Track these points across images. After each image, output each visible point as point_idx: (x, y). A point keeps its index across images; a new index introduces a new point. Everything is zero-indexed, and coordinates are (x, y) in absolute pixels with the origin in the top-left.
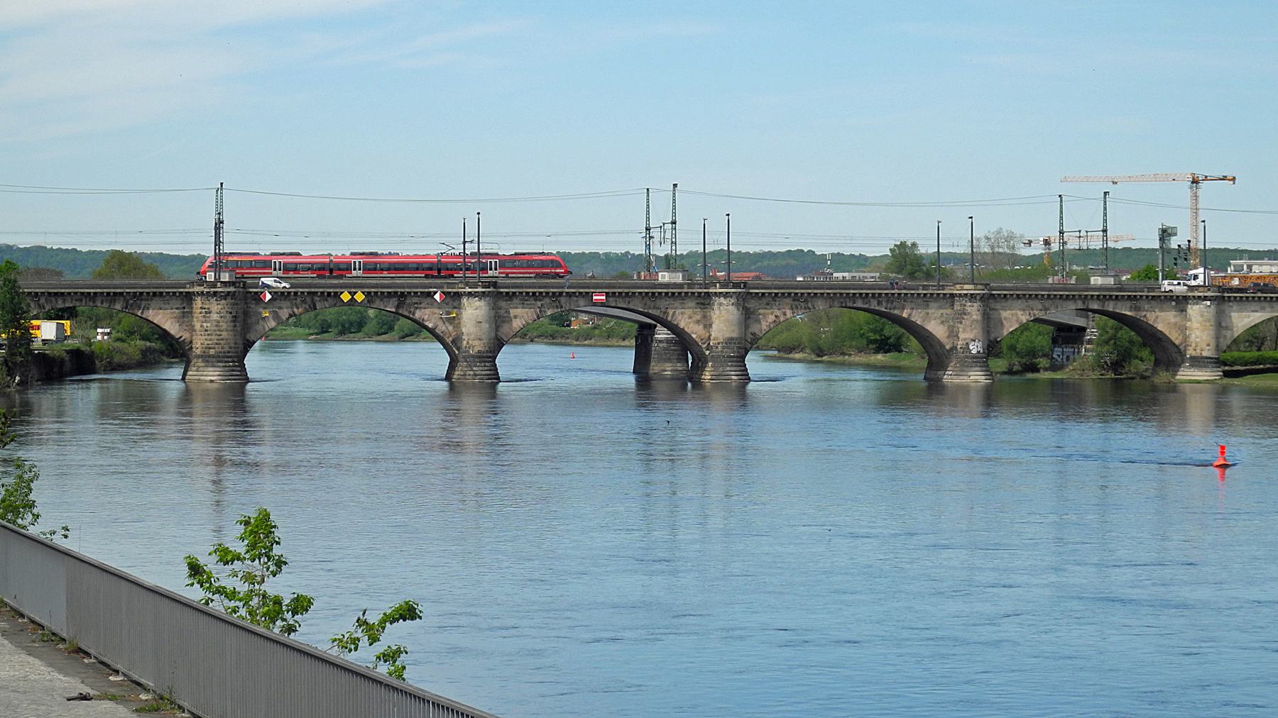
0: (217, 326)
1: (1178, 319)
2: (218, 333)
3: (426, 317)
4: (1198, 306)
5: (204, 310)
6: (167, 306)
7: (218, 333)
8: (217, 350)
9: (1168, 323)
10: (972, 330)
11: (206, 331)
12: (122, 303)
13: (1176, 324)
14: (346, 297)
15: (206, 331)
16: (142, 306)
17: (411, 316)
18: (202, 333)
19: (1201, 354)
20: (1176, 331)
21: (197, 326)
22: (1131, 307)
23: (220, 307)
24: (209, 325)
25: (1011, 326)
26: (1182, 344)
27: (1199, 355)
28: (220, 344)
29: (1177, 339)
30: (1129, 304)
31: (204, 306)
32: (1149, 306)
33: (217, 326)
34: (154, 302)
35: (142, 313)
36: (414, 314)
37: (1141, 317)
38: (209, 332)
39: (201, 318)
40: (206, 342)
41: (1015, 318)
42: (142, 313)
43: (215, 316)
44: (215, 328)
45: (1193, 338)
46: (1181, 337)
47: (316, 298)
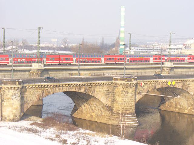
0: (131, 100)
2: (131, 103)
3: (191, 90)
5: (124, 92)
6: (102, 90)
7: (131, 103)
8: (130, 111)
11: (125, 102)
12: (84, 89)
14: (169, 83)
15: (125, 102)
16: (92, 90)
17: (186, 90)
18: (123, 103)
21: (119, 99)
23: (132, 90)
24: (127, 99)
28: (132, 108)
31: (124, 90)
33: (131, 100)
34: (97, 88)
35: (92, 93)
36: (187, 89)
38: (127, 103)
39: (122, 96)
40: (125, 108)
42: (92, 93)
43: (129, 95)
44: (130, 101)
47: (157, 84)
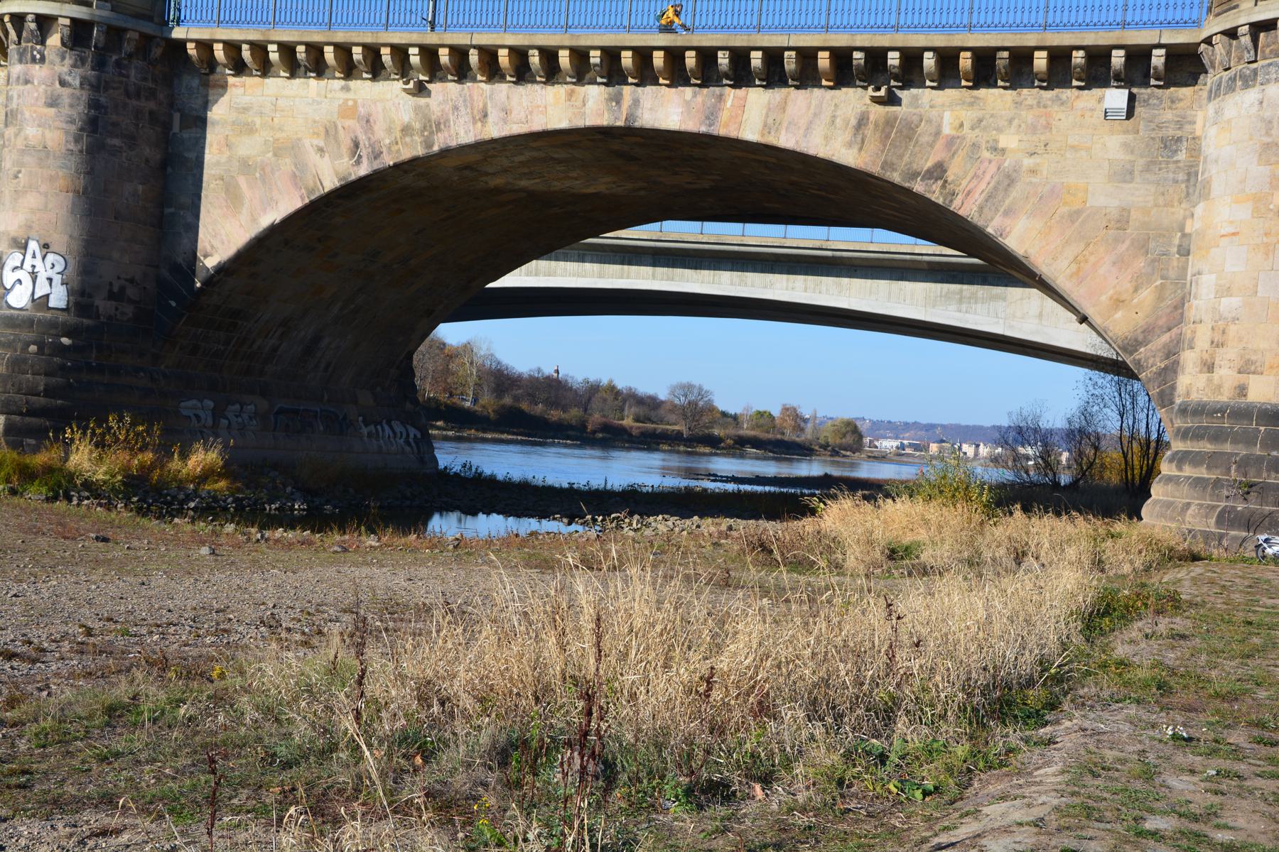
1: (1139, 194)
4: (1252, 95)
9: (1074, 216)
10: (17, 193)
13: (1122, 221)
19: (1242, 390)
20: (1120, 263)
22: (862, 122)
25: (269, 203)
26: (1149, 332)
27: (1225, 397)
29: (1118, 302)
30: (855, 100)
32: (968, 116)
37: (914, 175)
41: (287, 164)
45: (1203, 301)
46: (1147, 295)
